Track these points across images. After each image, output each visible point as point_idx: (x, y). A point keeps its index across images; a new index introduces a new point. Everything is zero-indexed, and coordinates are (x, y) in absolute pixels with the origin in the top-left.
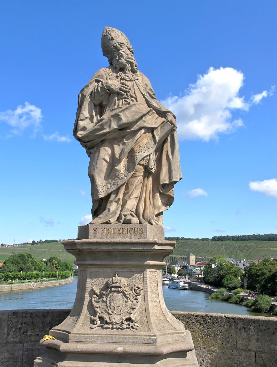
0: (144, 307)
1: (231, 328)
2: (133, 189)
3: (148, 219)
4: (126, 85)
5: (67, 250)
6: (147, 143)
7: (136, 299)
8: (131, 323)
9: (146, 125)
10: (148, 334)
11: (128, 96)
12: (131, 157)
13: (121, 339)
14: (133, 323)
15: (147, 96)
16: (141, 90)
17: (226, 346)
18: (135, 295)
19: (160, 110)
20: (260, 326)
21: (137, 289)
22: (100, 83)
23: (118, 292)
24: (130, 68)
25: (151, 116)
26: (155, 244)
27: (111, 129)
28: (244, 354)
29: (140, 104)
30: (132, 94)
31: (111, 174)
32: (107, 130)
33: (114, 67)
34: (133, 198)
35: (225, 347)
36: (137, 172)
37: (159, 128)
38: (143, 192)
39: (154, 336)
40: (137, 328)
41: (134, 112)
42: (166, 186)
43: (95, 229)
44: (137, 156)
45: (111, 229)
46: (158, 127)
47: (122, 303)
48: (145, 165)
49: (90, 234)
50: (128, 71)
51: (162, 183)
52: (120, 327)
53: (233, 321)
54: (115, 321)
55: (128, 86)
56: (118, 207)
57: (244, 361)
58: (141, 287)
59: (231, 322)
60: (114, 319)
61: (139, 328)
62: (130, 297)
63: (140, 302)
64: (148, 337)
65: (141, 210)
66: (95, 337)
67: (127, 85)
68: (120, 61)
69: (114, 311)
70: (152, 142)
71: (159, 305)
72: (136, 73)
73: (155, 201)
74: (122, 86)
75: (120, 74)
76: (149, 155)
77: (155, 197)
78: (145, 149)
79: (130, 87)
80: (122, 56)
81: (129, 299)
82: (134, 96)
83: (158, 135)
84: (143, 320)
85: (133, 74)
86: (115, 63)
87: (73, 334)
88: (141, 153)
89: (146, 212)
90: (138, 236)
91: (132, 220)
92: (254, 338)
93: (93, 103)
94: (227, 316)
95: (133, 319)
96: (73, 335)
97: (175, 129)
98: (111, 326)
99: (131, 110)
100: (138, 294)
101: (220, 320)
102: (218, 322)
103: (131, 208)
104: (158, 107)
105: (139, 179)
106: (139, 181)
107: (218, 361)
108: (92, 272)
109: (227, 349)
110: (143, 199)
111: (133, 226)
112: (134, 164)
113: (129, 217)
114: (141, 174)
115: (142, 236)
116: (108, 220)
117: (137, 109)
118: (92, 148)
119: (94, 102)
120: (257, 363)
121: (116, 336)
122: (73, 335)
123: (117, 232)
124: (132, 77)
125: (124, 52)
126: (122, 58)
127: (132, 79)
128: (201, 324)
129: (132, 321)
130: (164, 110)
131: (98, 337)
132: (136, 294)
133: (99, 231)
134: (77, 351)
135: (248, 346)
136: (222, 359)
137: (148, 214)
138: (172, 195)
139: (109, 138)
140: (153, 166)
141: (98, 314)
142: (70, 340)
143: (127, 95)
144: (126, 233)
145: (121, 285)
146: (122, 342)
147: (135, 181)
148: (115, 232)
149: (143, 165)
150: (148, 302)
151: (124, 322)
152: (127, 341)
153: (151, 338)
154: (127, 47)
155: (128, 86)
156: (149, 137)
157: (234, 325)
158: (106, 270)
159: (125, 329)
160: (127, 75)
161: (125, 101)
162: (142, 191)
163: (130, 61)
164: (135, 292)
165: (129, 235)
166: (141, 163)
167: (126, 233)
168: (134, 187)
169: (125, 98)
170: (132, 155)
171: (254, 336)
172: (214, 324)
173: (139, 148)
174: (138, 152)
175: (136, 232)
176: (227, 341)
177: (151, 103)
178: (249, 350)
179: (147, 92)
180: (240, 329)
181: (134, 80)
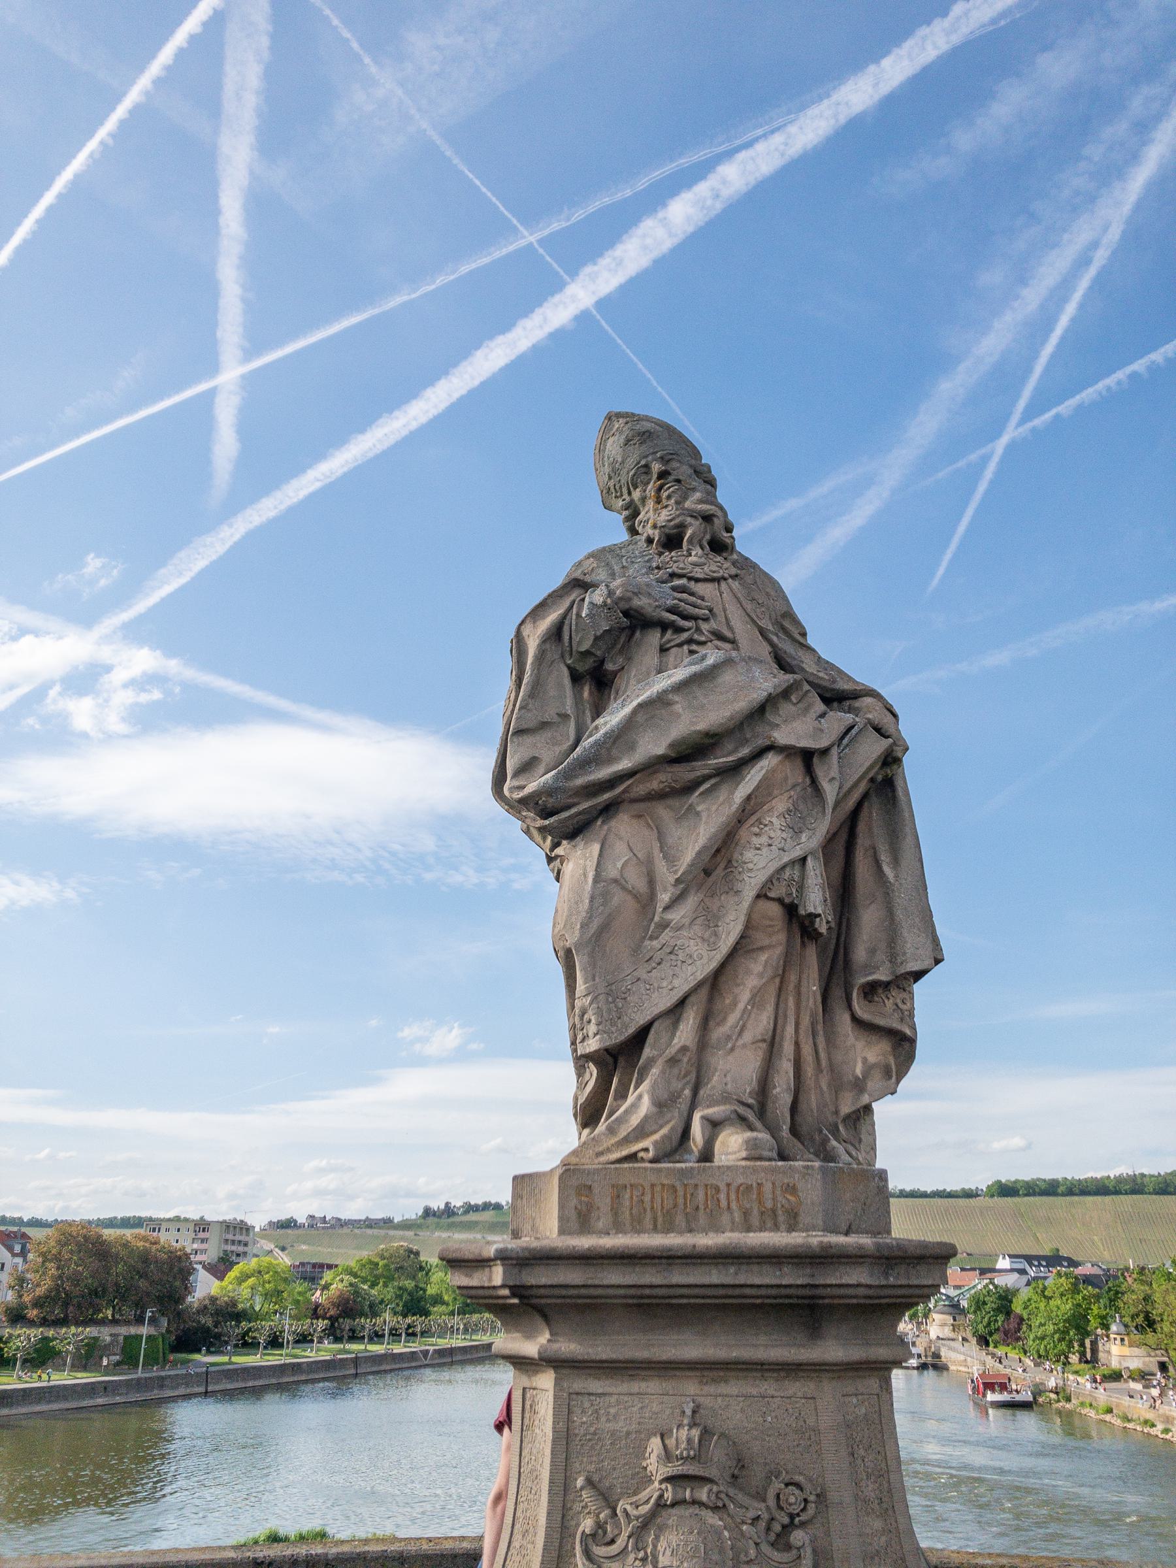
2: (741, 1006)
4: (692, 594)
5: (465, 1292)
9: (782, 736)
12: (726, 868)
25: (800, 705)
31: (647, 943)
37: (834, 751)
38: (785, 1016)
46: (832, 745)
55: (703, 599)
76: (803, 860)
78: (784, 835)
82: (728, 634)
83: (833, 779)
85: (719, 558)
88: (765, 850)
89: (803, 1106)
90: (781, 1218)
93: (569, 667)
97: (899, 755)
99: (720, 680)
105: (766, 962)
106: (765, 967)
110: (788, 1048)
119: (569, 662)
123: (681, 1201)
127: (715, 575)
133: (603, 1202)
138: (908, 1032)
139: (632, 795)
143: (698, 630)
144: (724, 1203)
149: (780, 901)
155: (703, 599)
156: (798, 789)
162: (780, 1012)
165: (737, 1216)
166: (772, 894)
167: (724, 1203)
169: (690, 641)
170: (730, 861)
175: (769, 1204)
181: (725, 579)
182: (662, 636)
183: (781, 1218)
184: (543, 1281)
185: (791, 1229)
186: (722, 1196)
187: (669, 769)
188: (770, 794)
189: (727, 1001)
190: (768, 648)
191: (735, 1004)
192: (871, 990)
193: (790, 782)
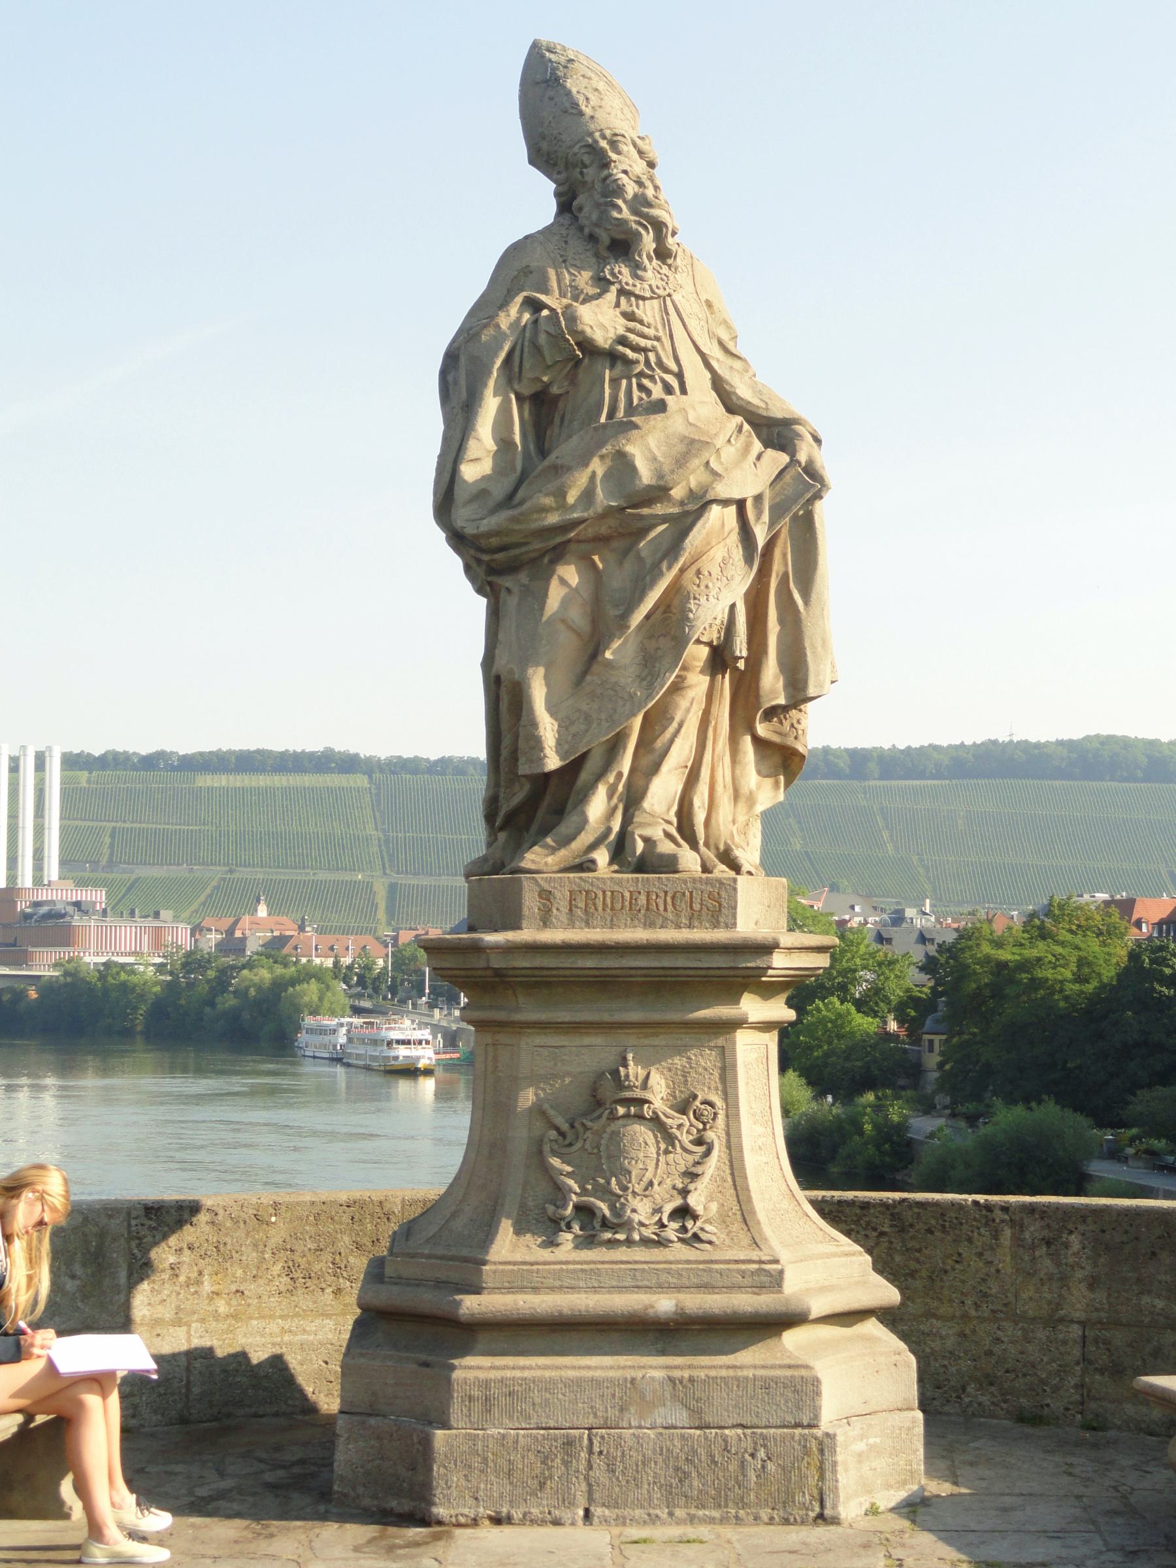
0: (728, 1171)
1: (998, 1246)
3: (722, 847)
4: (641, 322)
5: (440, 972)
6: (724, 559)
7: (699, 1142)
8: (689, 1224)
10: (755, 1255)
11: (653, 370)
12: (665, 612)
13: (664, 1277)
14: (699, 1224)
15: (718, 360)
16: (696, 338)
17: (977, 1310)
18: (698, 1130)
19: (765, 414)
20: (1103, 1231)
21: (703, 1107)
22: (545, 313)
23: (640, 1117)
24: (654, 246)
26: (767, 948)
27: (591, 512)
28: (1041, 1334)
29: (702, 402)
30: (665, 360)
31: (588, 678)
33: (587, 231)
34: (670, 771)
35: (973, 1313)
36: (686, 673)
39: (777, 1262)
40: (713, 1239)
41: (682, 441)
42: (779, 711)
43: (546, 895)
44: (691, 611)
45: (604, 892)
47: (655, 1156)
48: (715, 643)
49: (526, 911)
50: (644, 256)
51: (767, 705)
52: (655, 1237)
53: (1007, 1217)
54: (636, 1218)
56: (615, 808)
57: (1042, 1360)
58: (719, 1102)
59: (998, 1221)
60: (634, 1211)
61: (718, 1238)
62: (682, 1134)
63: (715, 1153)
64: (756, 1266)
65: (700, 817)
66: (574, 1271)
67: (646, 320)
68: (615, 214)
69: (630, 1185)
70: (738, 554)
71: (776, 1160)
72: (670, 261)
73: (738, 772)
74: (629, 330)
75: (616, 271)
77: (740, 757)
78: (719, 584)
79: (657, 330)
80: (619, 191)
81: (679, 1141)
84: (730, 1214)
85: (665, 269)
86: (589, 215)
87: (495, 1263)
88: (703, 600)
89: (713, 821)
90: (704, 917)
91: (680, 861)
92: (1079, 1274)
94: (982, 1201)
95: (699, 1210)
96: (493, 1267)
98: (621, 1237)
100: (708, 1127)
101: (956, 1218)
102: (947, 1224)
103: (664, 809)
104: (755, 401)
105: (693, 699)
107: (945, 1366)
108: (536, 1049)
109: (982, 1320)
111: (685, 882)
112: (680, 643)
113: (666, 847)
114: (699, 683)
115: (718, 921)
116: (584, 858)
117: (690, 429)
118: (512, 568)
119: (516, 387)
120: (1090, 1362)
121: (645, 1266)
122: (493, 1267)
123: (627, 904)
124: (660, 283)
125: (625, 172)
126: (620, 202)
128: (882, 1234)
129: (695, 1218)
130: (779, 415)
131: (582, 1270)
132: (701, 1126)
134: (520, 1319)
135: (1058, 1304)
136: (960, 1358)
137: (719, 830)
140: (741, 647)
141: (574, 1197)
142: (484, 1285)
143: (647, 363)
144: (661, 908)
145: (648, 1095)
146: (667, 1285)
147: (677, 706)
148: (618, 906)
149: (710, 644)
150: (741, 1151)
151: (665, 1221)
152: (685, 1282)
153: (765, 1270)
154: (635, 145)
157: (1008, 1232)
158: (587, 1040)
159: (672, 1242)
160: (640, 273)
161: (641, 387)
163: (652, 217)
164: (697, 1119)
165: (670, 915)
167: (661, 908)
168: (671, 730)
171: (1083, 1268)
172: (932, 1233)
173: (698, 582)
174: (695, 598)
175: (697, 907)
176: (981, 1291)
177: (732, 386)
178: (1061, 1320)
179: (711, 335)
180: (1033, 1247)
181: (669, 295)
185: (715, 925)
187: (618, 516)
188: (709, 543)
190: (709, 376)
192: (772, 713)
193: (727, 529)
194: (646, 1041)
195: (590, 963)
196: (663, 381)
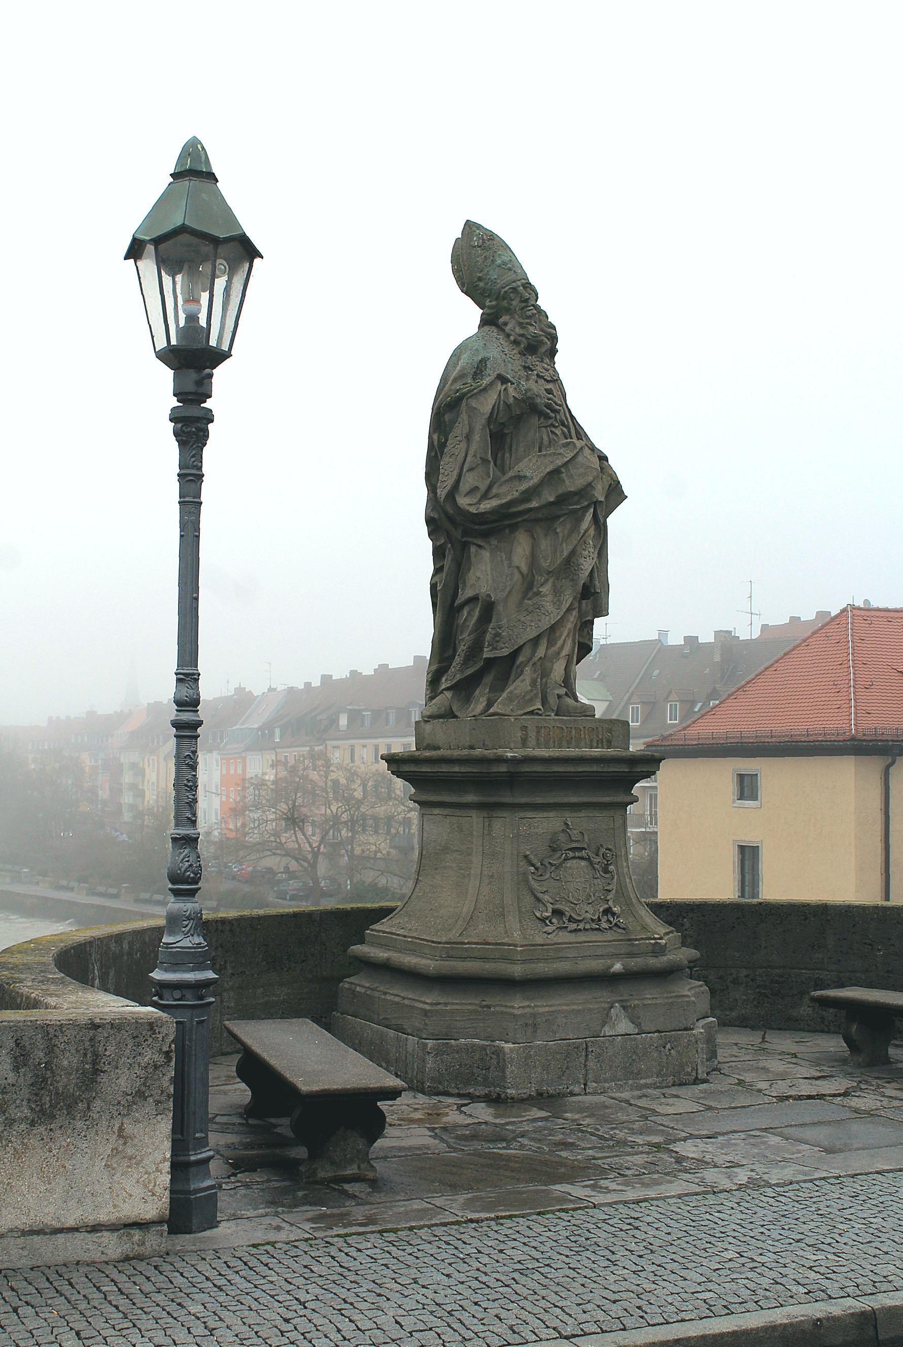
2: (563, 637)
32: (534, 504)
60: (586, 912)
66: (566, 948)
133: (532, 734)
158: (545, 814)
182: (539, 420)
183: (605, 743)
184: (527, 770)
186: (582, 732)
189: (557, 635)
191: (560, 636)
194: (574, 815)
195: (561, 769)
196: (562, 430)
